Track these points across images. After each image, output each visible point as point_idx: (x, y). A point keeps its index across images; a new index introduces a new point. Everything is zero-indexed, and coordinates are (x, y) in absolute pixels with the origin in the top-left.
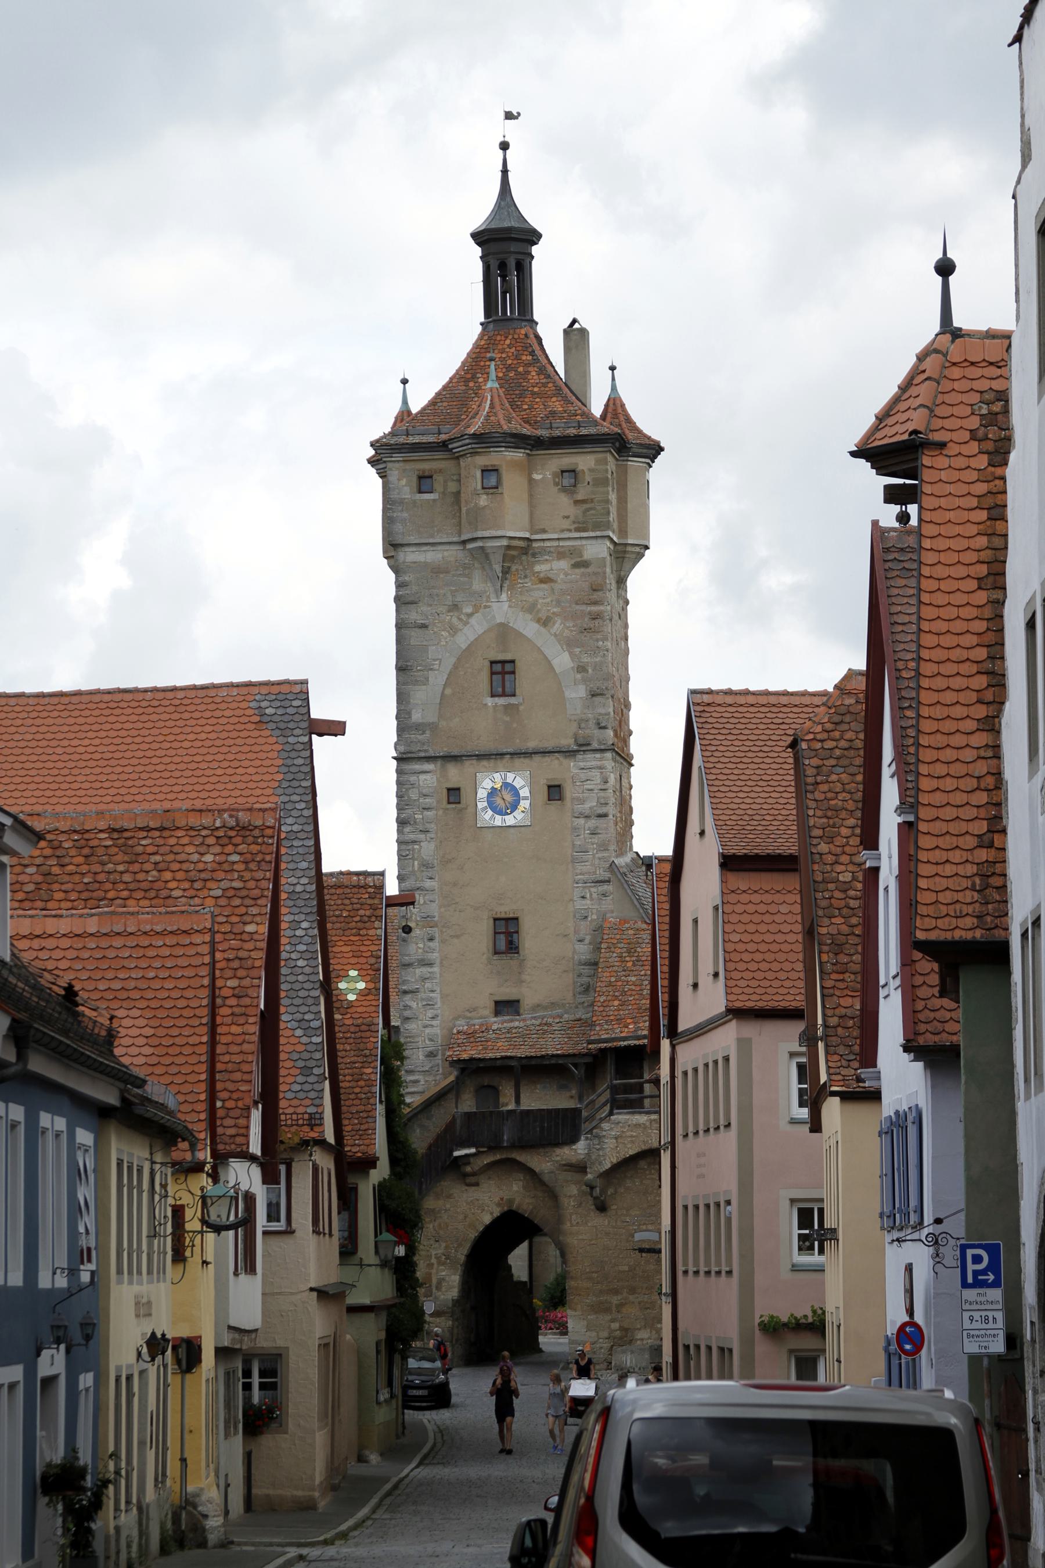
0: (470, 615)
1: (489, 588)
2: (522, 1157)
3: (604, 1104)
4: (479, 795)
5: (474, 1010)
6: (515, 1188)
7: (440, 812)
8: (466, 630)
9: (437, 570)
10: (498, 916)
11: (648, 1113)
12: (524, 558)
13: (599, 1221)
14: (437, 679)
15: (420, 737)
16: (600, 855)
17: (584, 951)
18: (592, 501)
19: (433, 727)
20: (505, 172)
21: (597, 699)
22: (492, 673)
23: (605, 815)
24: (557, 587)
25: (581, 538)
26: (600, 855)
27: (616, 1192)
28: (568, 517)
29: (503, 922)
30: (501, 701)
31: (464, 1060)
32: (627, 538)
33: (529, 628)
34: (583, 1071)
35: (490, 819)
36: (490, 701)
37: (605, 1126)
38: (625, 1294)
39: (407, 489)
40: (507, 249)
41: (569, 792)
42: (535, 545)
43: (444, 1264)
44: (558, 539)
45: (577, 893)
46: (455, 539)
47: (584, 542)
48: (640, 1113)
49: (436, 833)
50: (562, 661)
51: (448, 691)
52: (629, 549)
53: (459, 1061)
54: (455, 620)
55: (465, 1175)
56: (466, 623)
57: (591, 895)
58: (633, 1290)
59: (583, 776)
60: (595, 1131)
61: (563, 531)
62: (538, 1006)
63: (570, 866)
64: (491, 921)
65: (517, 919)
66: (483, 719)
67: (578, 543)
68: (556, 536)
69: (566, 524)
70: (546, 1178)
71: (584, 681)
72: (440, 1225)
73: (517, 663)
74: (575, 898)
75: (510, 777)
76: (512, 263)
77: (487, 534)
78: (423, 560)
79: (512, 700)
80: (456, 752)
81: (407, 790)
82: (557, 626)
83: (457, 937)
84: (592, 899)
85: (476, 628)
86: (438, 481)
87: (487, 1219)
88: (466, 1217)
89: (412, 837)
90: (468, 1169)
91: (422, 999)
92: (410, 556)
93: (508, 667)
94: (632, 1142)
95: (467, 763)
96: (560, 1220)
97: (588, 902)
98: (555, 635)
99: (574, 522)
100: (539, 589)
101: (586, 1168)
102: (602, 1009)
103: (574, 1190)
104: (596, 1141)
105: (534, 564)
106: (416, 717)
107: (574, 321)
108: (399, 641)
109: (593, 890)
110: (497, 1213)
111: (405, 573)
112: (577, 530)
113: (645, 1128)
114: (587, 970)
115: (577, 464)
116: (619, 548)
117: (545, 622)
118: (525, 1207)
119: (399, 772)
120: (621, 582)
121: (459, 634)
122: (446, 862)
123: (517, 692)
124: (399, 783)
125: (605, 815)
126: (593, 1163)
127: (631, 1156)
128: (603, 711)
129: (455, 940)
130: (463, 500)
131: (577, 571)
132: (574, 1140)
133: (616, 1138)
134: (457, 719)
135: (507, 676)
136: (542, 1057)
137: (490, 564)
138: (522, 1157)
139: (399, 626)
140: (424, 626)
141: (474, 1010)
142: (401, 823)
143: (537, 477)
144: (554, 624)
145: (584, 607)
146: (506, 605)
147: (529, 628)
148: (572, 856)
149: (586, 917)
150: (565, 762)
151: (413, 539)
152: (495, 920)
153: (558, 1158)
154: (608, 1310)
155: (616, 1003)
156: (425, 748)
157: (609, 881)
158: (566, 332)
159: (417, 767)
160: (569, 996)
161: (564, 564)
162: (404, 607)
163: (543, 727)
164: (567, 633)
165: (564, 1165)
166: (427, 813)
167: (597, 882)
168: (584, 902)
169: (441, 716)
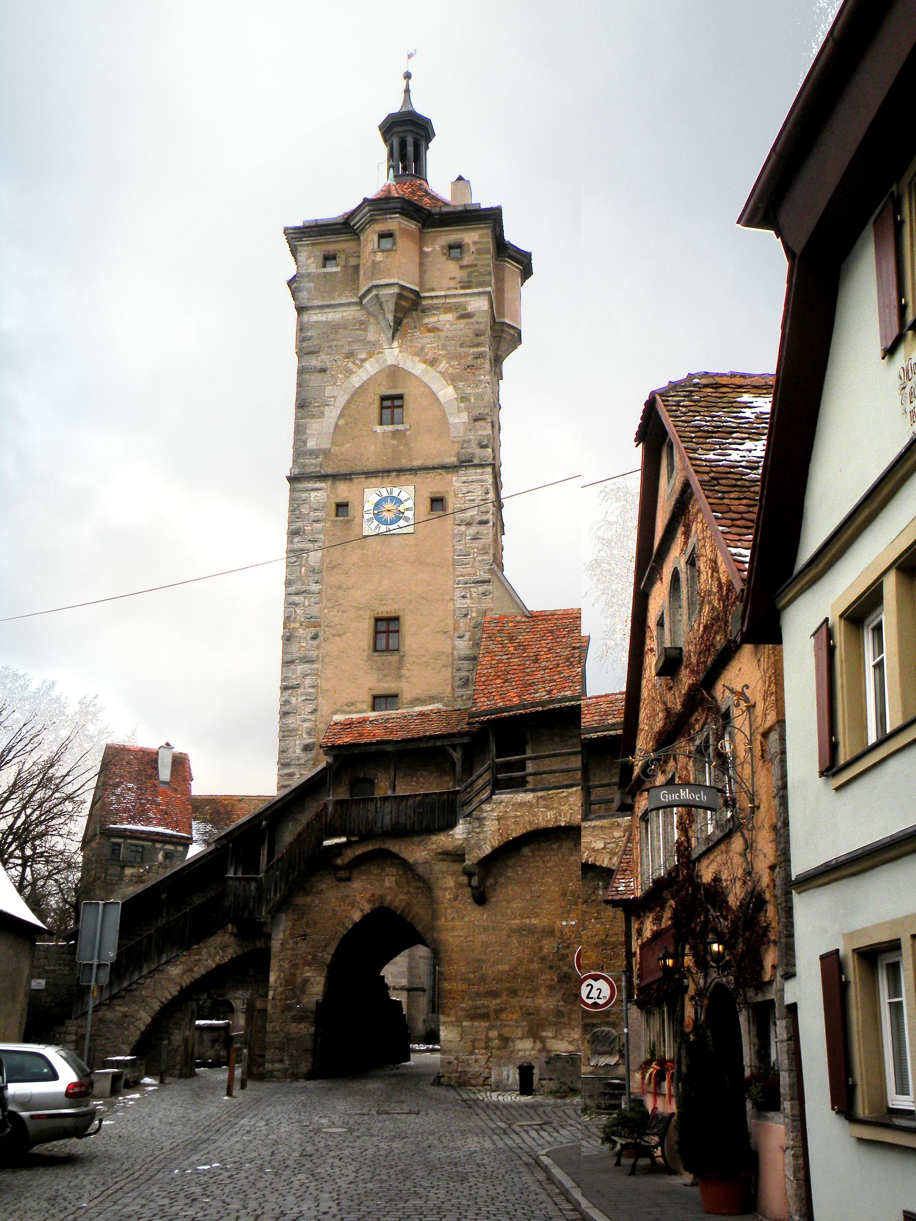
0: (363, 361)
1: (384, 337)
2: (394, 847)
3: (483, 788)
4: (366, 508)
5: (352, 704)
6: (387, 884)
7: (329, 524)
8: (360, 372)
9: (335, 327)
10: (380, 615)
11: (533, 790)
12: (414, 313)
13: (477, 915)
14: (332, 414)
15: (313, 461)
16: (480, 558)
17: (463, 646)
18: (476, 265)
19: (326, 453)
20: (407, 91)
21: (477, 423)
22: (382, 408)
23: (486, 522)
24: (442, 334)
25: (466, 295)
26: (480, 558)
27: (496, 882)
28: (453, 279)
29: (384, 623)
30: (390, 428)
31: (339, 746)
32: (504, 317)
33: (417, 368)
34: (460, 753)
35: (376, 528)
36: (379, 429)
37: (487, 807)
38: (504, 998)
39: (314, 265)
40: (407, 135)
41: (452, 504)
42: (425, 302)
43: (309, 965)
44: (445, 296)
45: (458, 594)
46: (355, 300)
47: (468, 299)
48: (526, 791)
49: (324, 543)
50: (446, 393)
51: (342, 422)
52: (506, 328)
53: (333, 747)
54: (350, 365)
55: (338, 868)
56: (360, 367)
57: (471, 594)
58: (513, 992)
59: (465, 490)
60: (474, 813)
61: (449, 289)
62: (417, 699)
63: (451, 569)
64: (373, 621)
65: (397, 619)
66: (373, 442)
67: (463, 299)
68: (443, 293)
69: (452, 284)
70: (420, 870)
71: (467, 409)
72: (307, 923)
73: (406, 397)
74: (455, 598)
75: (396, 492)
76: (410, 140)
77: (382, 282)
78: (324, 319)
79: (401, 427)
80: (344, 470)
81: (299, 505)
82: (443, 365)
83: (340, 635)
84: (471, 598)
85: (370, 368)
86: (341, 260)
87: (357, 916)
88: (335, 915)
89: (301, 546)
90: (339, 861)
91: (302, 695)
92: (315, 317)
93: (397, 402)
94: (516, 823)
95: (356, 481)
96: (435, 916)
97: (468, 601)
98: (441, 372)
99: (460, 282)
100: (426, 337)
101: (464, 855)
102: (483, 687)
103: (450, 882)
104: (476, 824)
105: (421, 319)
106: (311, 444)
107: (460, 178)
108: (299, 385)
109: (473, 590)
110: (367, 908)
111: (308, 330)
112: (462, 288)
113: (531, 806)
114: (466, 665)
115: (463, 239)
116: (497, 327)
117: (432, 363)
118: (397, 903)
119: (292, 491)
120: (497, 361)
121: (354, 375)
122: (332, 568)
123: (405, 421)
124: (292, 500)
125: (486, 522)
126: (472, 849)
127: (514, 839)
128: (484, 433)
129: (338, 639)
130: (361, 266)
131: (461, 321)
132: (452, 825)
133: (499, 819)
134: (348, 445)
135: (396, 410)
136: (420, 739)
137: (384, 314)
138: (394, 847)
139: (301, 371)
140: (323, 370)
141: (352, 704)
142: (293, 533)
143: (428, 249)
144: (440, 364)
145: (467, 349)
146: (397, 351)
147: (417, 368)
148: (453, 559)
149: (466, 615)
150: (449, 476)
151: (317, 303)
152: (377, 620)
153: (434, 846)
154: (484, 1016)
155: (499, 681)
156: (318, 469)
157: (489, 582)
158: (453, 183)
159: (311, 485)
160: (448, 690)
161: (449, 317)
162: (305, 357)
163: (427, 448)
164: (451, 370)
165: (440, 854)
166: (315, 525)
167: (477, 582)
168: (464, 601)
169: (333, 443)
